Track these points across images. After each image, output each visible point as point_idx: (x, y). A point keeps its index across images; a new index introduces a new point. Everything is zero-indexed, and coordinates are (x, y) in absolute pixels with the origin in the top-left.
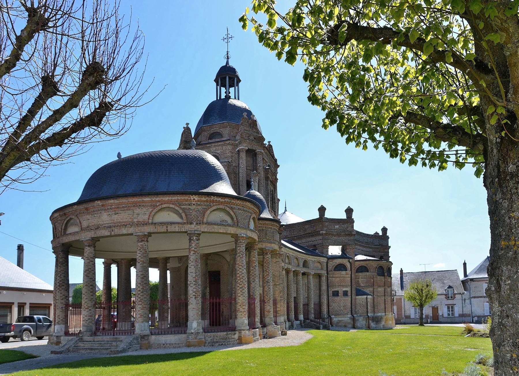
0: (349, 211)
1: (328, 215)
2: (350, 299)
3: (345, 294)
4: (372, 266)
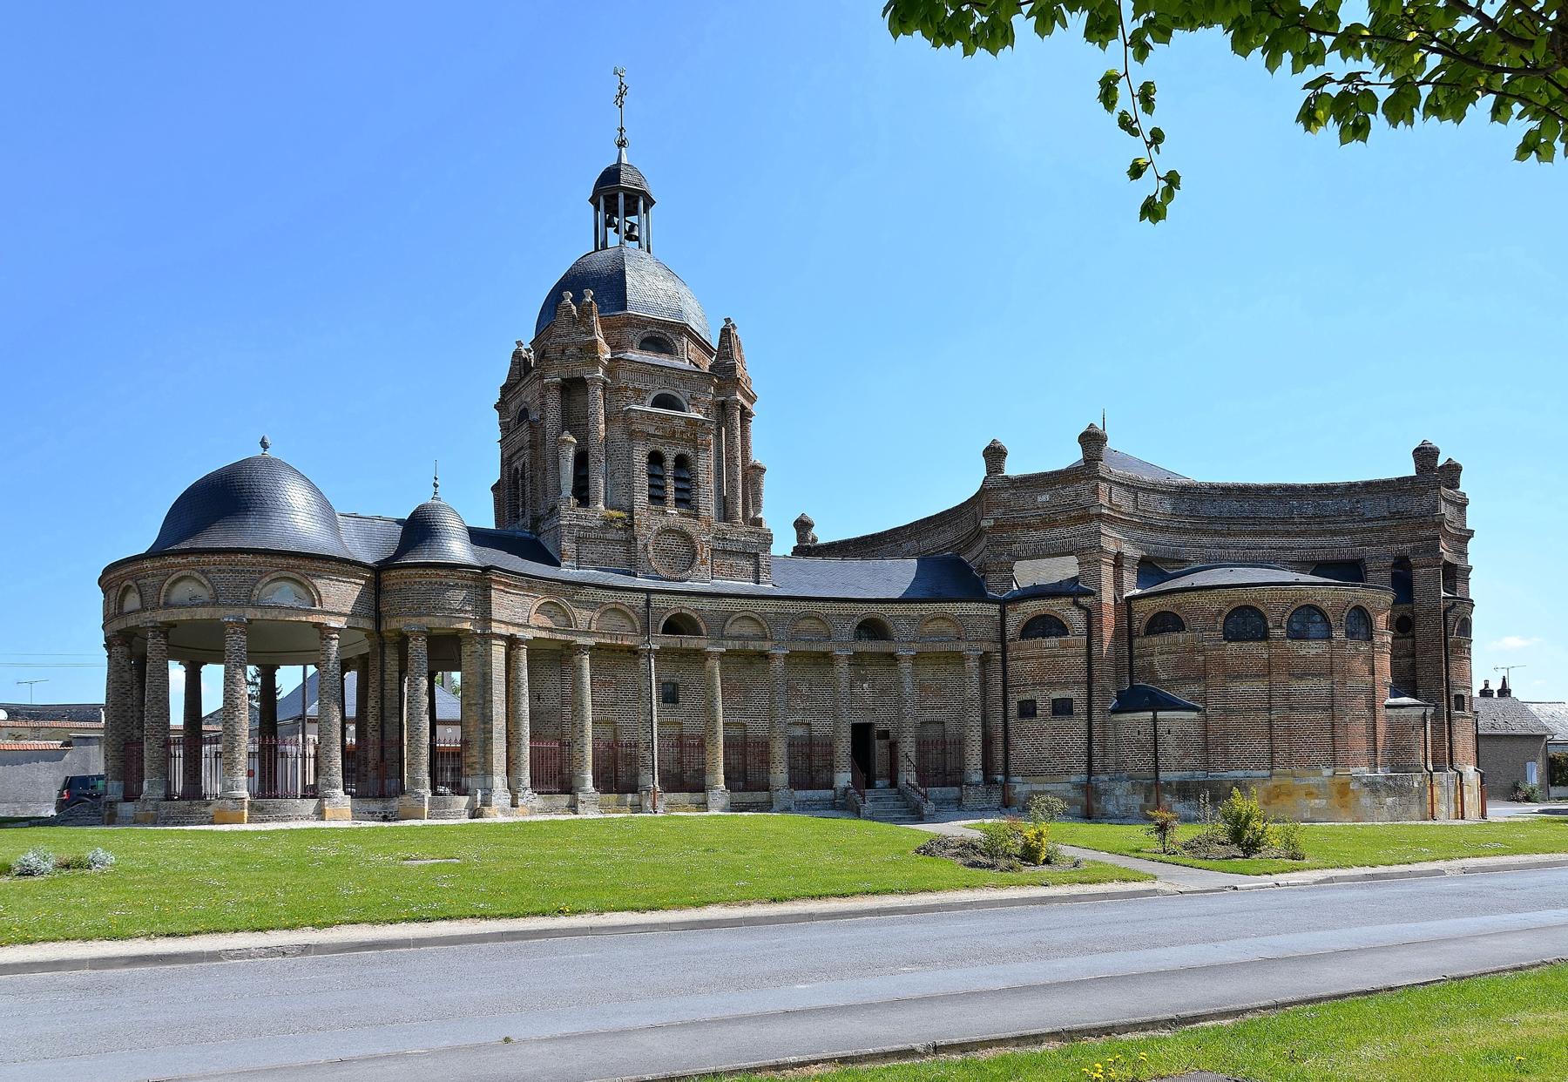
2: (1083, 725)
3: (1062, 708)
4: (1202, 609)
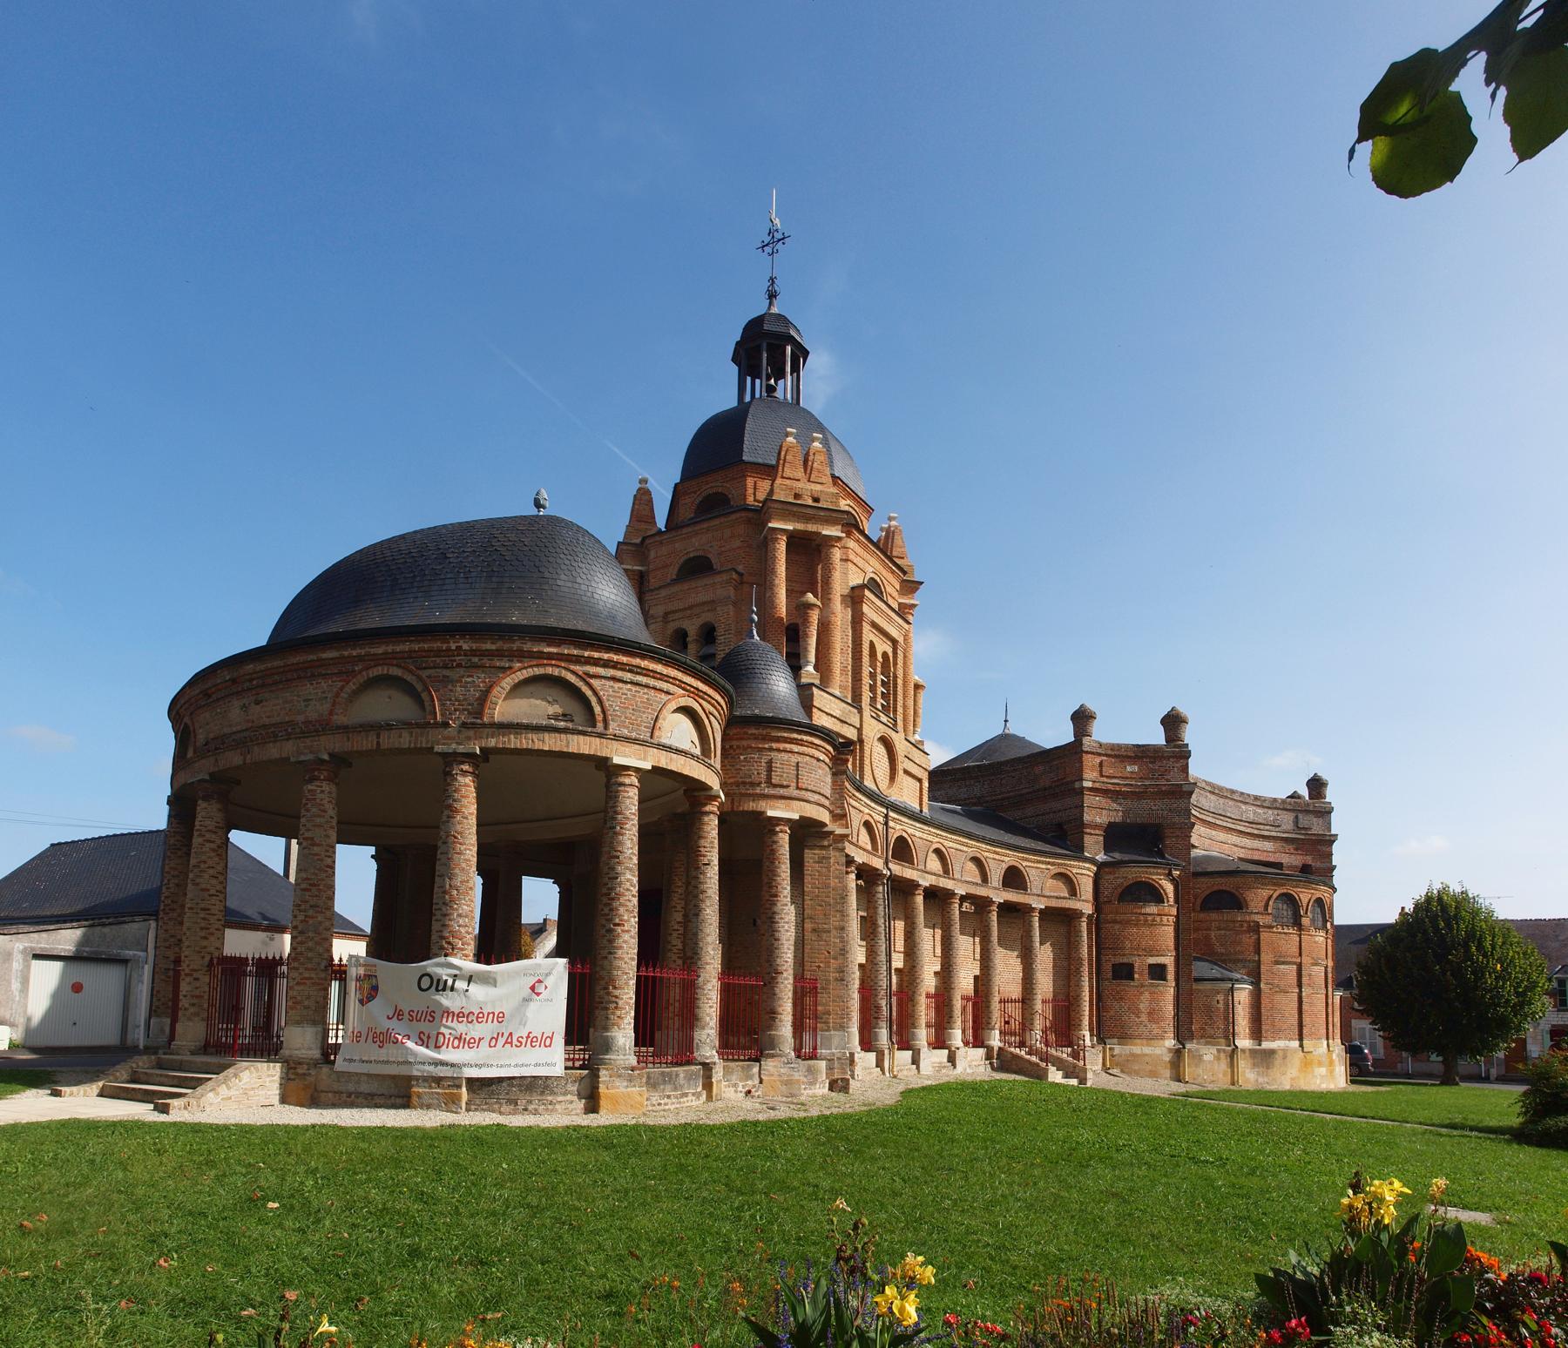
0: (1173, 722)
1: (1103, 733)
